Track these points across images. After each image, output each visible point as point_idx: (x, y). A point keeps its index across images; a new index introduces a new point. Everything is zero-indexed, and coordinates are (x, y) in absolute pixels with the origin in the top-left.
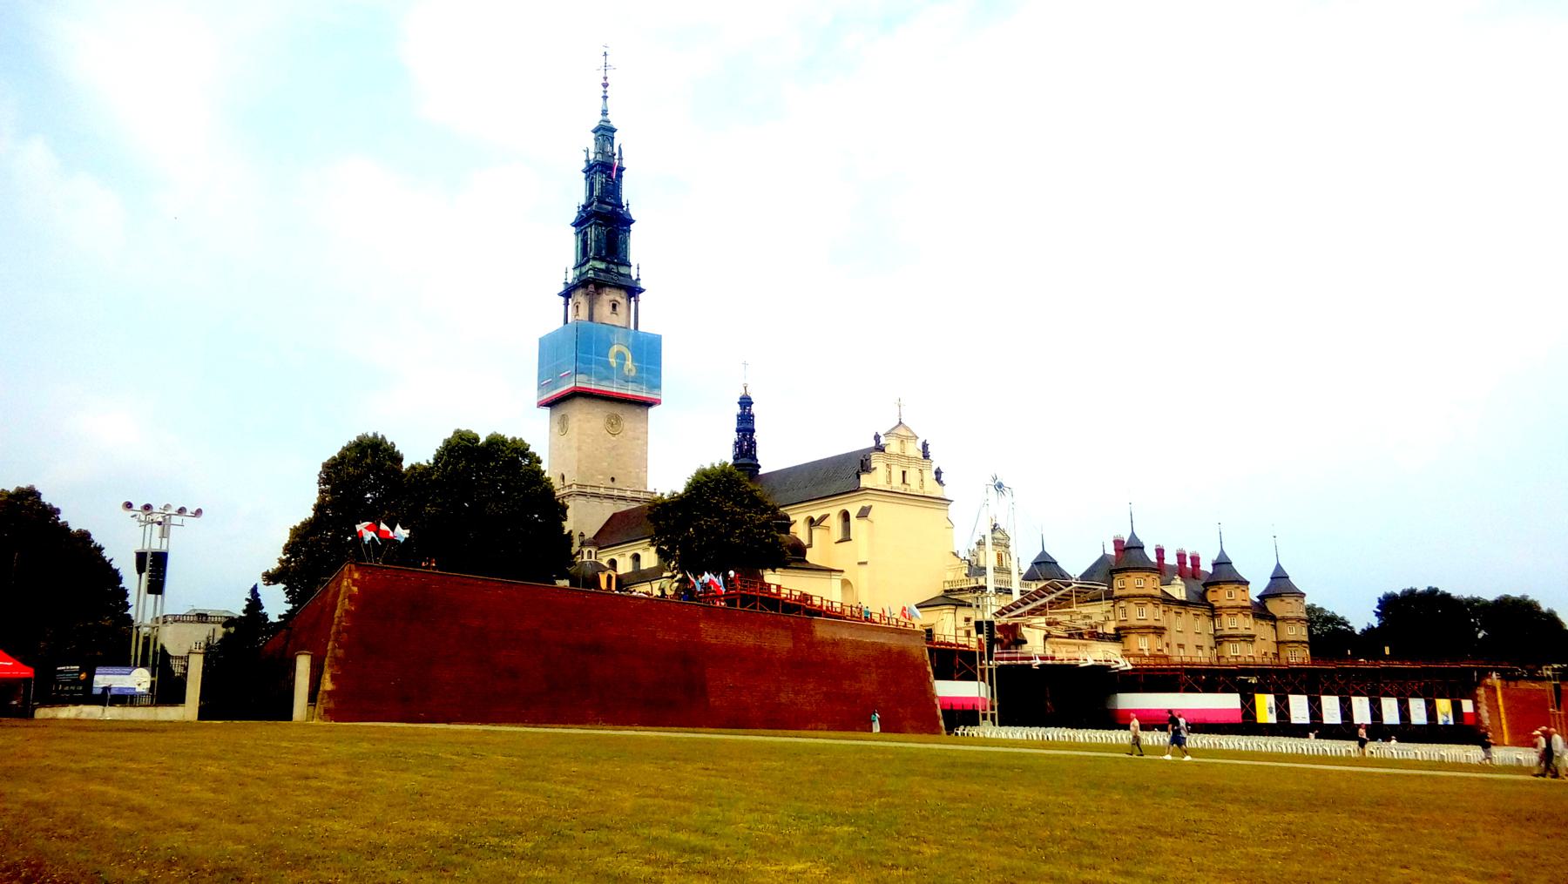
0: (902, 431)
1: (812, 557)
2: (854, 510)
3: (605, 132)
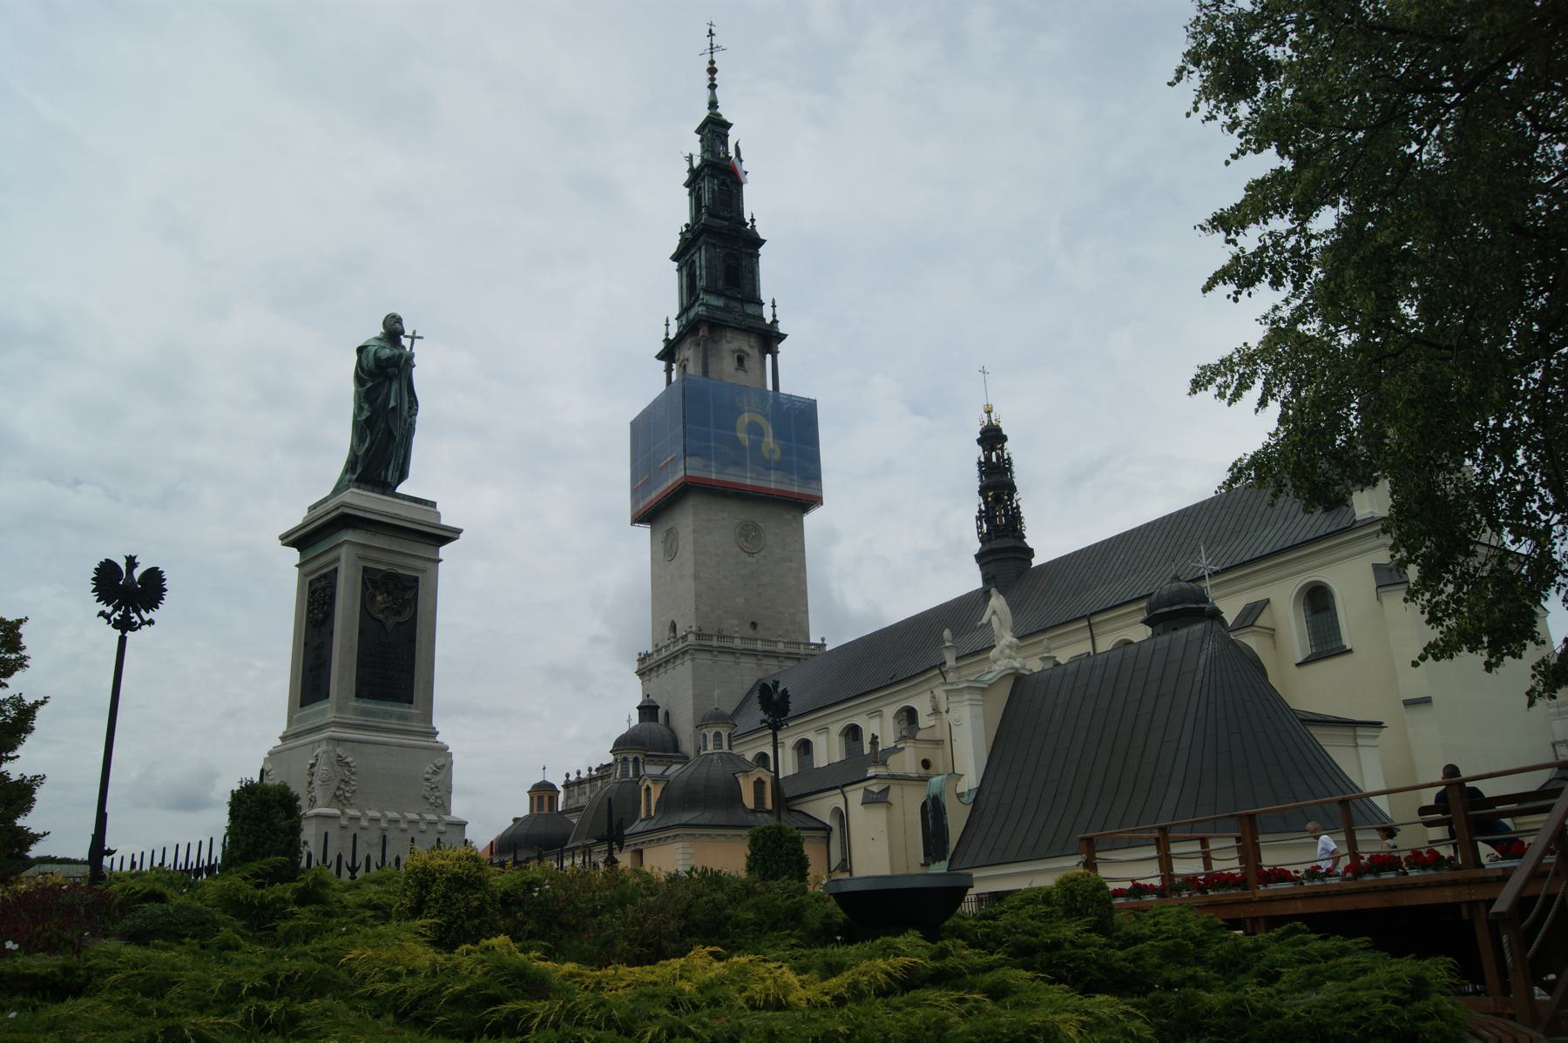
3: (714, 129)
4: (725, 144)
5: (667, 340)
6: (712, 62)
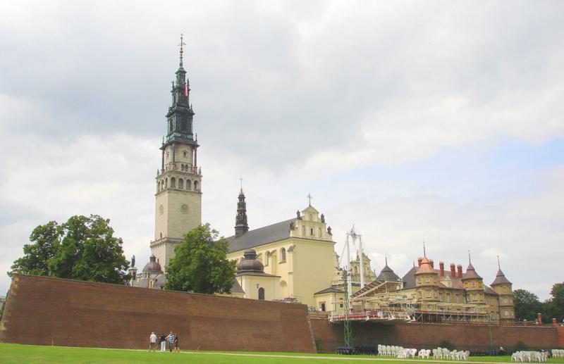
0: (311, 210)
1: (267, 270)
2: (287, 247)
3: (181, 74)
4: (184, 80)
5: (163, 144)
6: (182, 49)
